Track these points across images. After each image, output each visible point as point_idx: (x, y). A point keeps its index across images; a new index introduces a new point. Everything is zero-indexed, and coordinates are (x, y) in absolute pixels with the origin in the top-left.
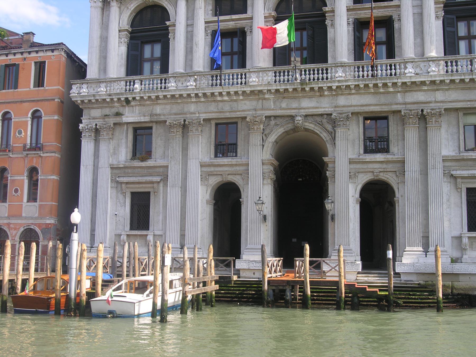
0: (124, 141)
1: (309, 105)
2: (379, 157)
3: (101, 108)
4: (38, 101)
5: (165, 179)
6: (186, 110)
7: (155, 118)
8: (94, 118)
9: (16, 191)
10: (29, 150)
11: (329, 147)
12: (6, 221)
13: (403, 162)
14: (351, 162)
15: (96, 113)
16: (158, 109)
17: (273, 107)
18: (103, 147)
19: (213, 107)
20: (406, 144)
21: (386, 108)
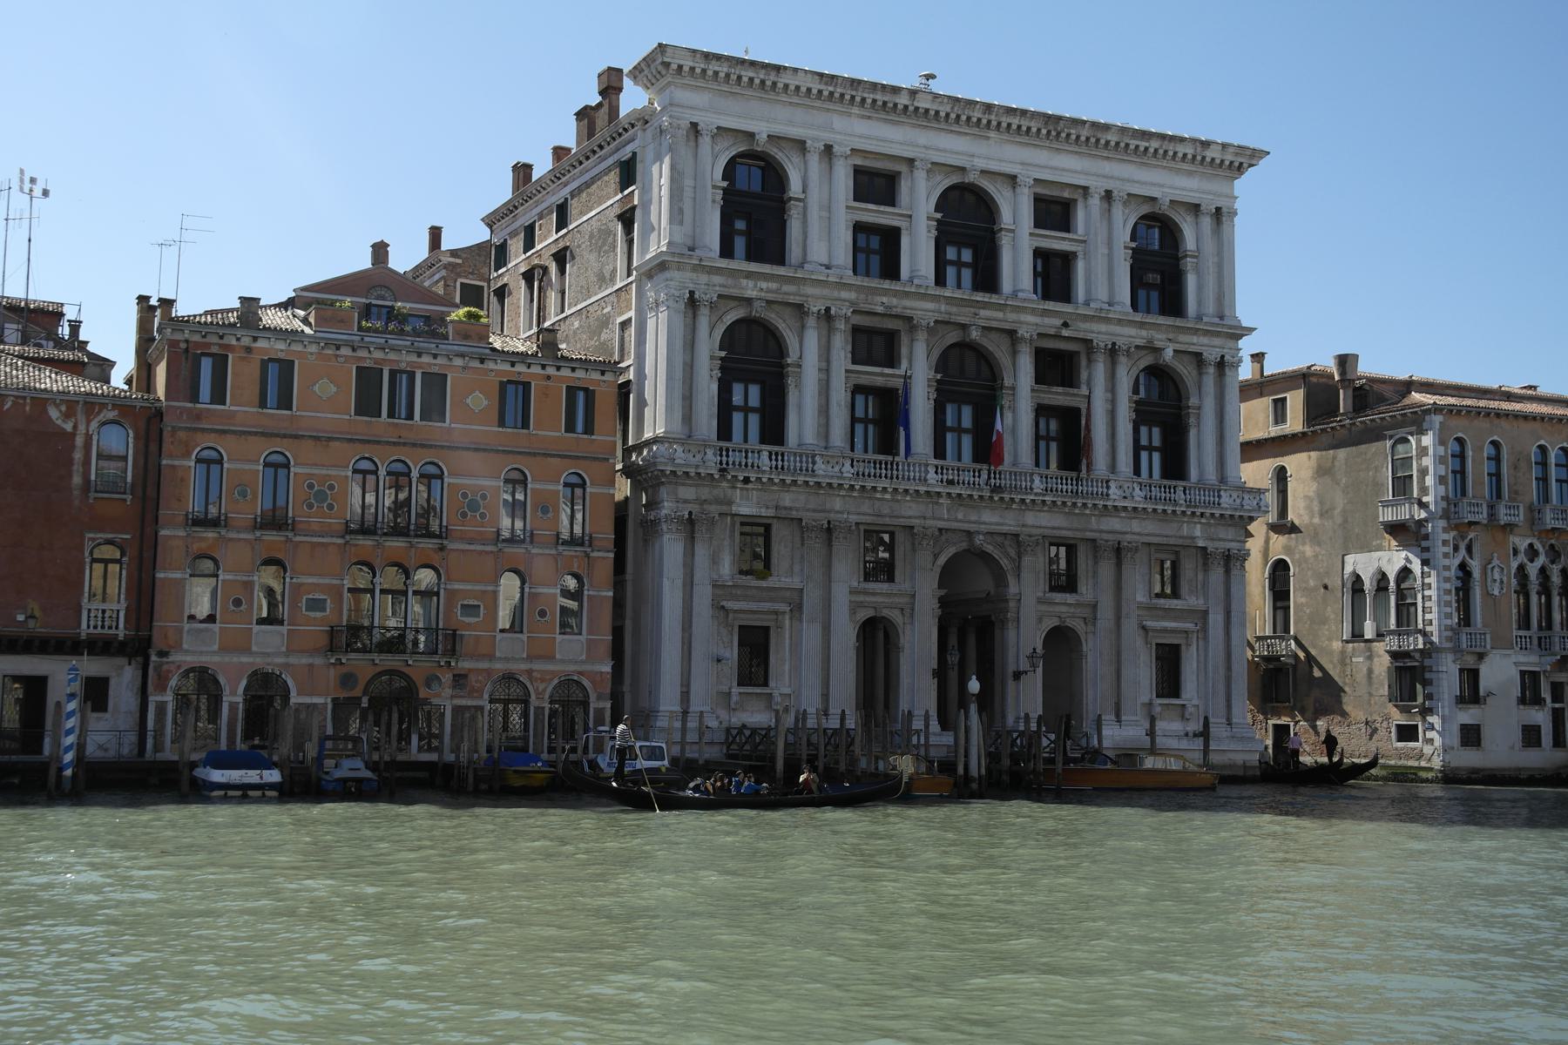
0: (726, 543)
1: (991, 518)
2: (1070, 598)
3: (697, 486)
4: (577, 458)
5: (797, 608)
6: (828, 506)
7: (783, 513)
8: (686, 501)
9: (542, 613)
10: (565, 543)
11: (1011, 580)
12: (523, 666)
13: (1095, 607)
14: (1040, 601)
15: (687, 492)
16: (787, 499)
17: (946, 515)
18: (701, 552)
19: (866, 507)
20: (1095, 585)
21: (1079, 535)
